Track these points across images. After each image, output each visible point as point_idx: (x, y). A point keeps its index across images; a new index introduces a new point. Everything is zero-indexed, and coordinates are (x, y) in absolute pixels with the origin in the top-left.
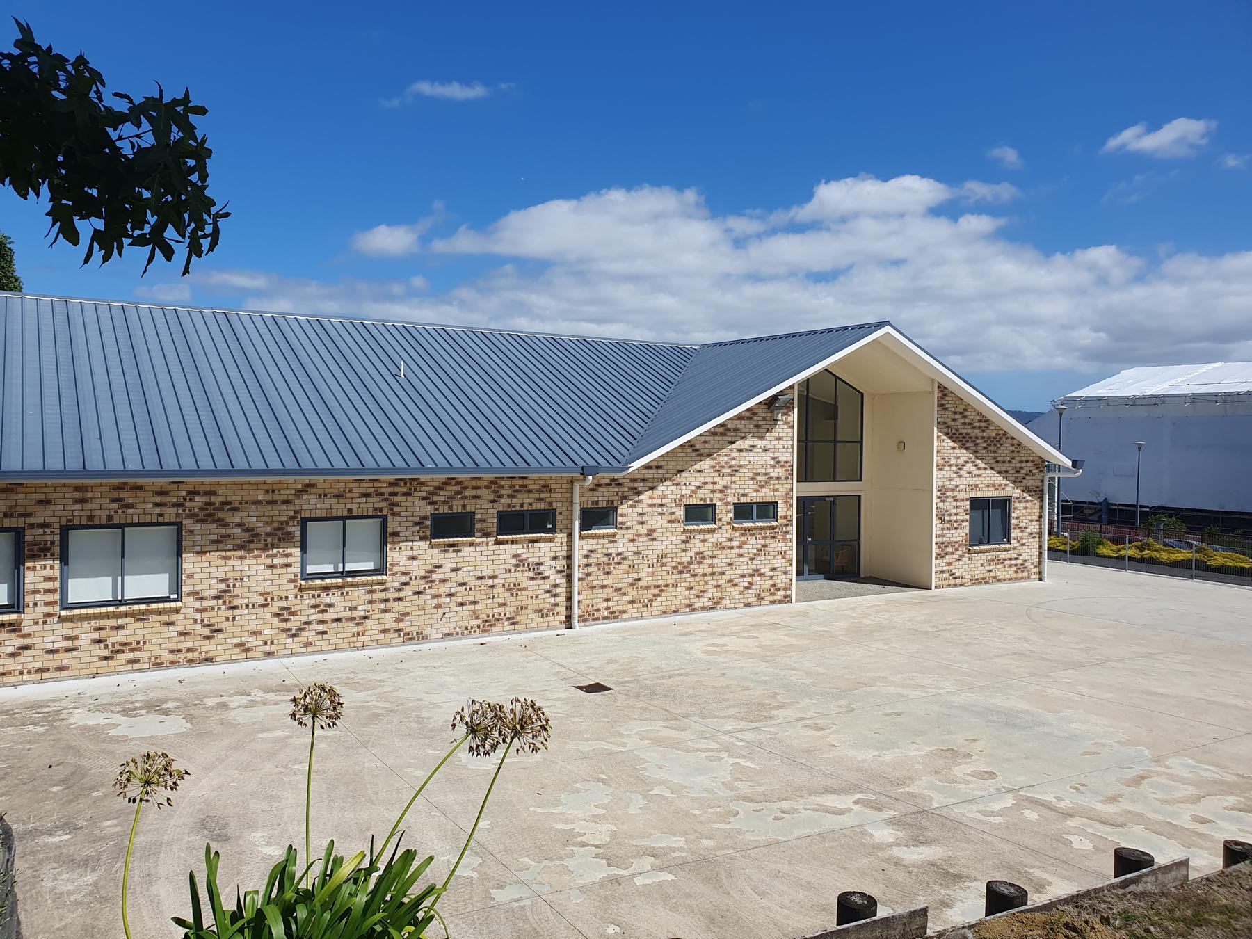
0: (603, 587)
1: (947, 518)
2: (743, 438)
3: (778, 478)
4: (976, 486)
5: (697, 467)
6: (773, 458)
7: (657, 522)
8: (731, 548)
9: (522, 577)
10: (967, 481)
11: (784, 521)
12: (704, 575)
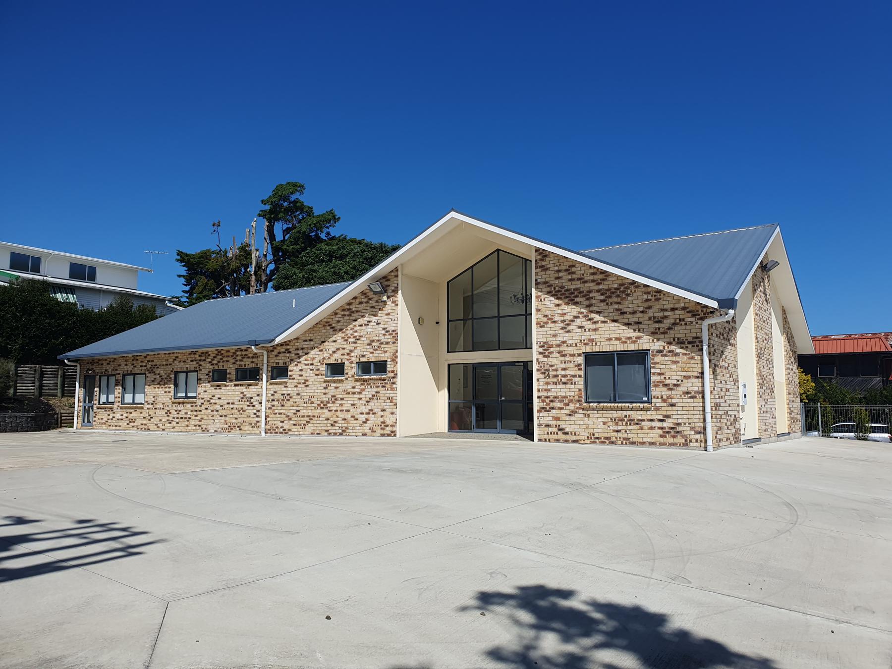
0: (280, 414)
1: (552, 373)
2: (362, 317)
3: (387, 343)
4: (591, 340)
5: (333, 339)
6: (384, 329)
7: (309, 375)
8: (354, 393)
9: (244, 404)
10: (576, 335)
11: (392, 375)
12: (336, 411)
